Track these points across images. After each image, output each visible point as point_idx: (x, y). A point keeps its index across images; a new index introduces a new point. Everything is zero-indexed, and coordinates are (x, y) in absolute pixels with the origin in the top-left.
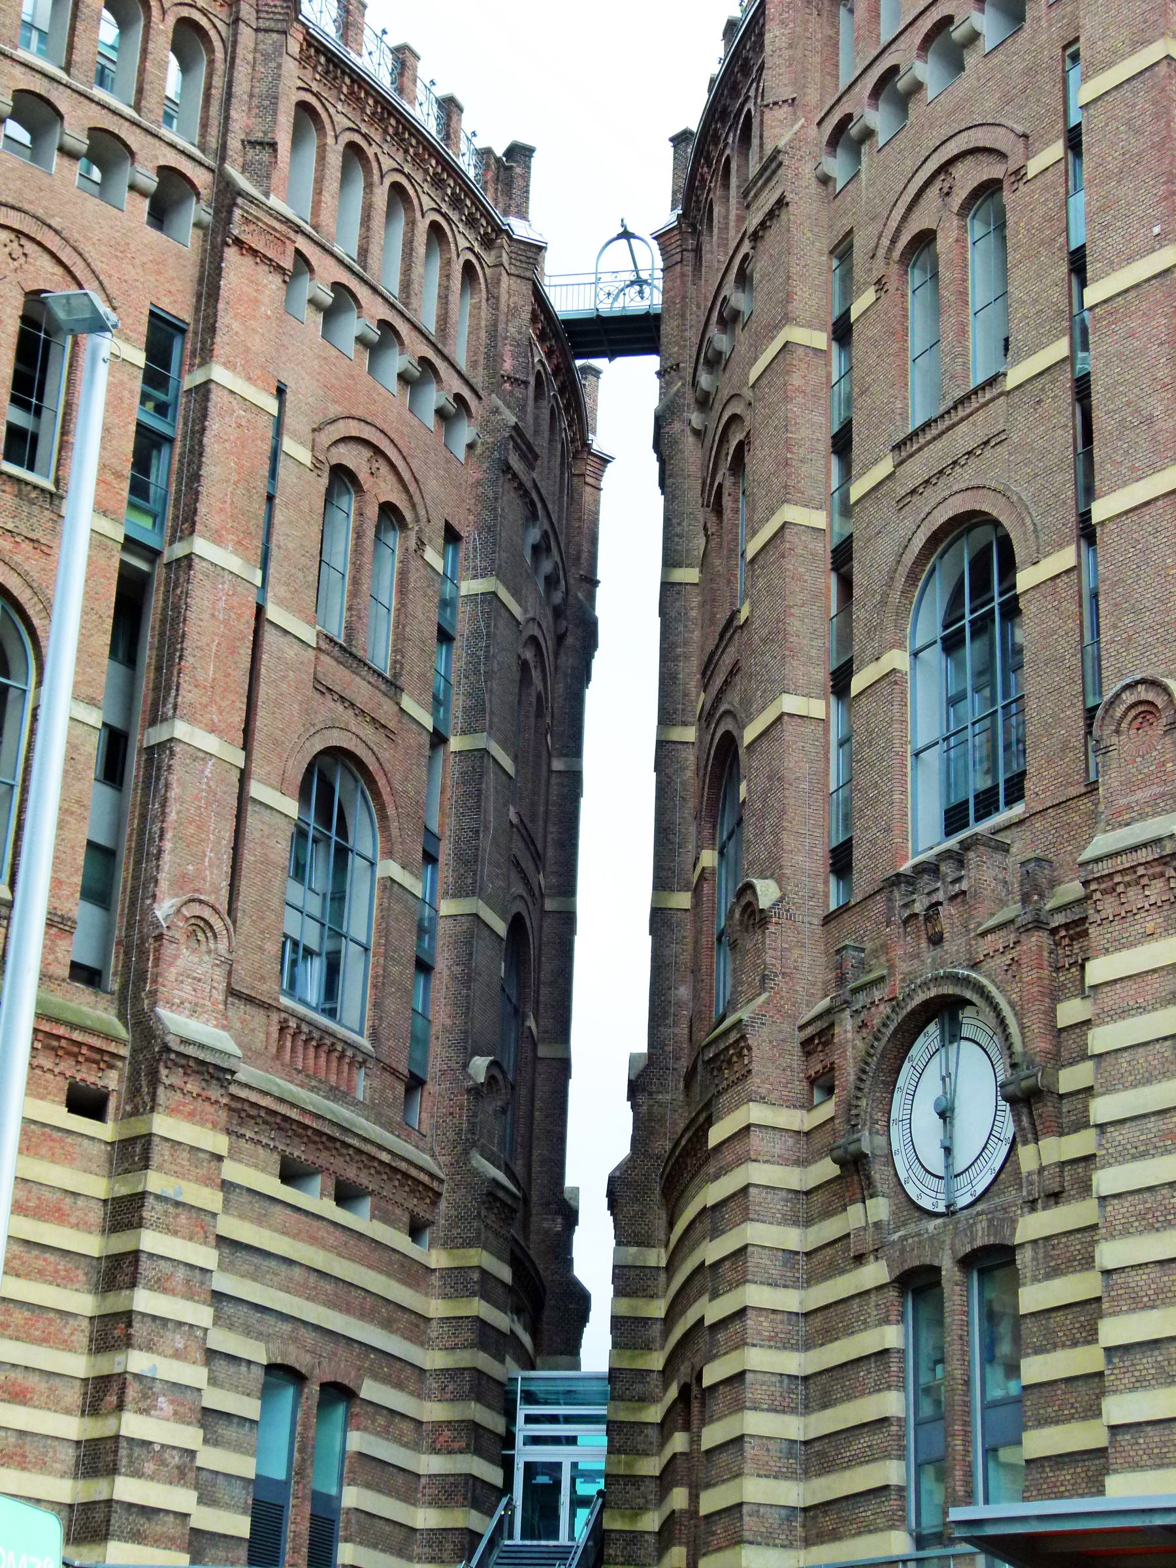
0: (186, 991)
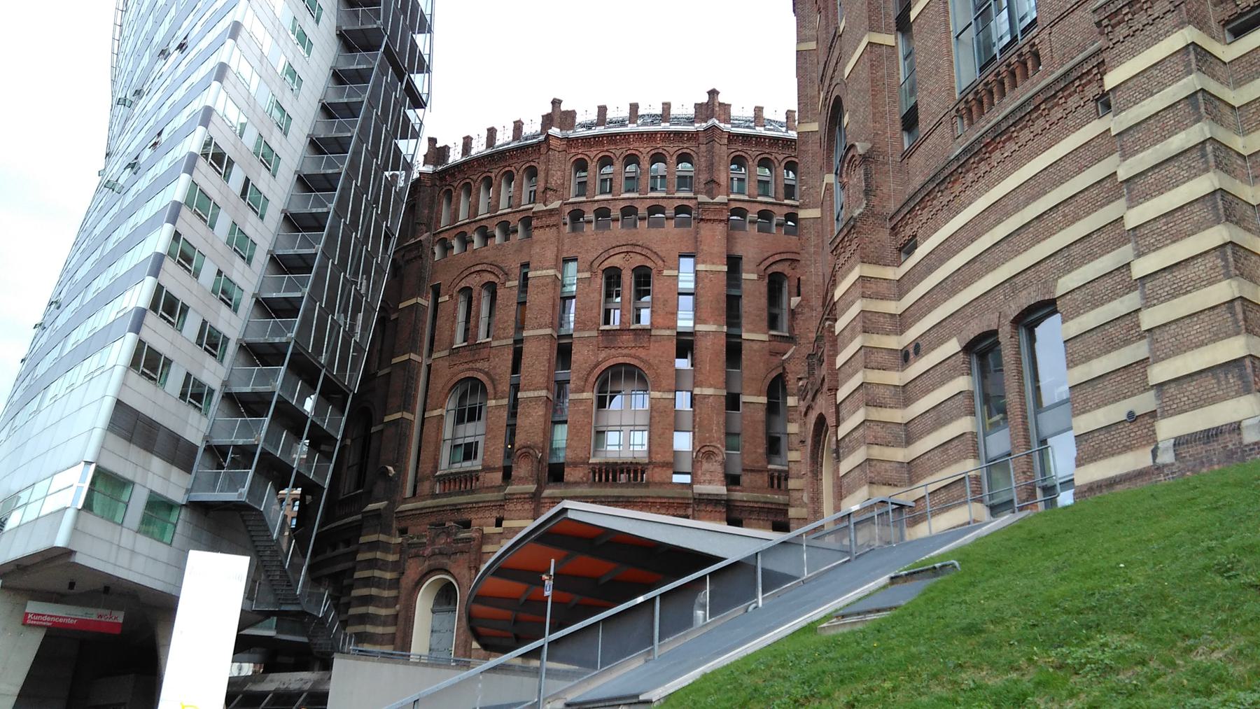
0: (708, 477)
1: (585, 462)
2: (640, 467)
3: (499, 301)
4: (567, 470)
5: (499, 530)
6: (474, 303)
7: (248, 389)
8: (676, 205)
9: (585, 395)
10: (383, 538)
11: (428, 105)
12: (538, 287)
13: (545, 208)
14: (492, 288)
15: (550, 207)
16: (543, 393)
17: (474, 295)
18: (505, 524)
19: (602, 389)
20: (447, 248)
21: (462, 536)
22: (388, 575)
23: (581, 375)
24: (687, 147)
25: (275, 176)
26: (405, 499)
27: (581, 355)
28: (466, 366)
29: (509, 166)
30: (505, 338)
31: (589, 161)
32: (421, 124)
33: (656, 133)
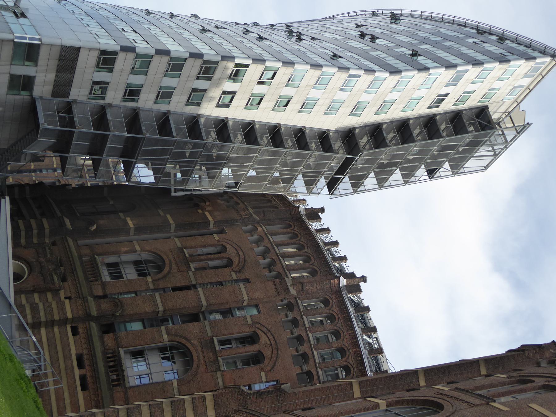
1: (119, 346)
2: (122, 382)
3: (220, 270)
4: (111, 335)
5: (63, 298)
6: (216, 256)
7: (109, 117)
8: (312, 371)
9: (165, 337)
10: (47, 231)
11: (333, 196)
13: (289, 285)
14: (230, 263)
15: (291, 288)
16: (161, 308)
17: (222, 255)
18: (67, 302)
19: (172, 348)
20: (251, 232)
21: (55, 278)
22: (23, 241)
23: (179, 331)
24: (354, 369)
25: (23, 15)
26: (76, 241)
27: (193, 328)
28: (172, 259)
29: (314, 259)
30: (196, 279)
31: (328, 308)
32: (319, 194)
33: (359, 347)
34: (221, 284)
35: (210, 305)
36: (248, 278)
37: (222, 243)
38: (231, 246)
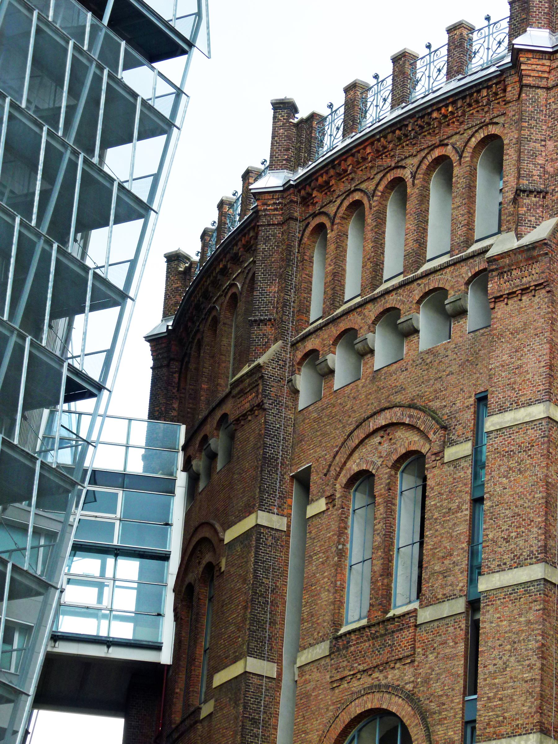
11: (201, 42)
12: (510, 454)
13: (515, 244)
28: (367, 681)
30: (447, 598)
32: (179, 92)
34: (478, 501)
35: (545, 549)
36: (472, 400)
37: (338, 486)
38: (356, 455)
